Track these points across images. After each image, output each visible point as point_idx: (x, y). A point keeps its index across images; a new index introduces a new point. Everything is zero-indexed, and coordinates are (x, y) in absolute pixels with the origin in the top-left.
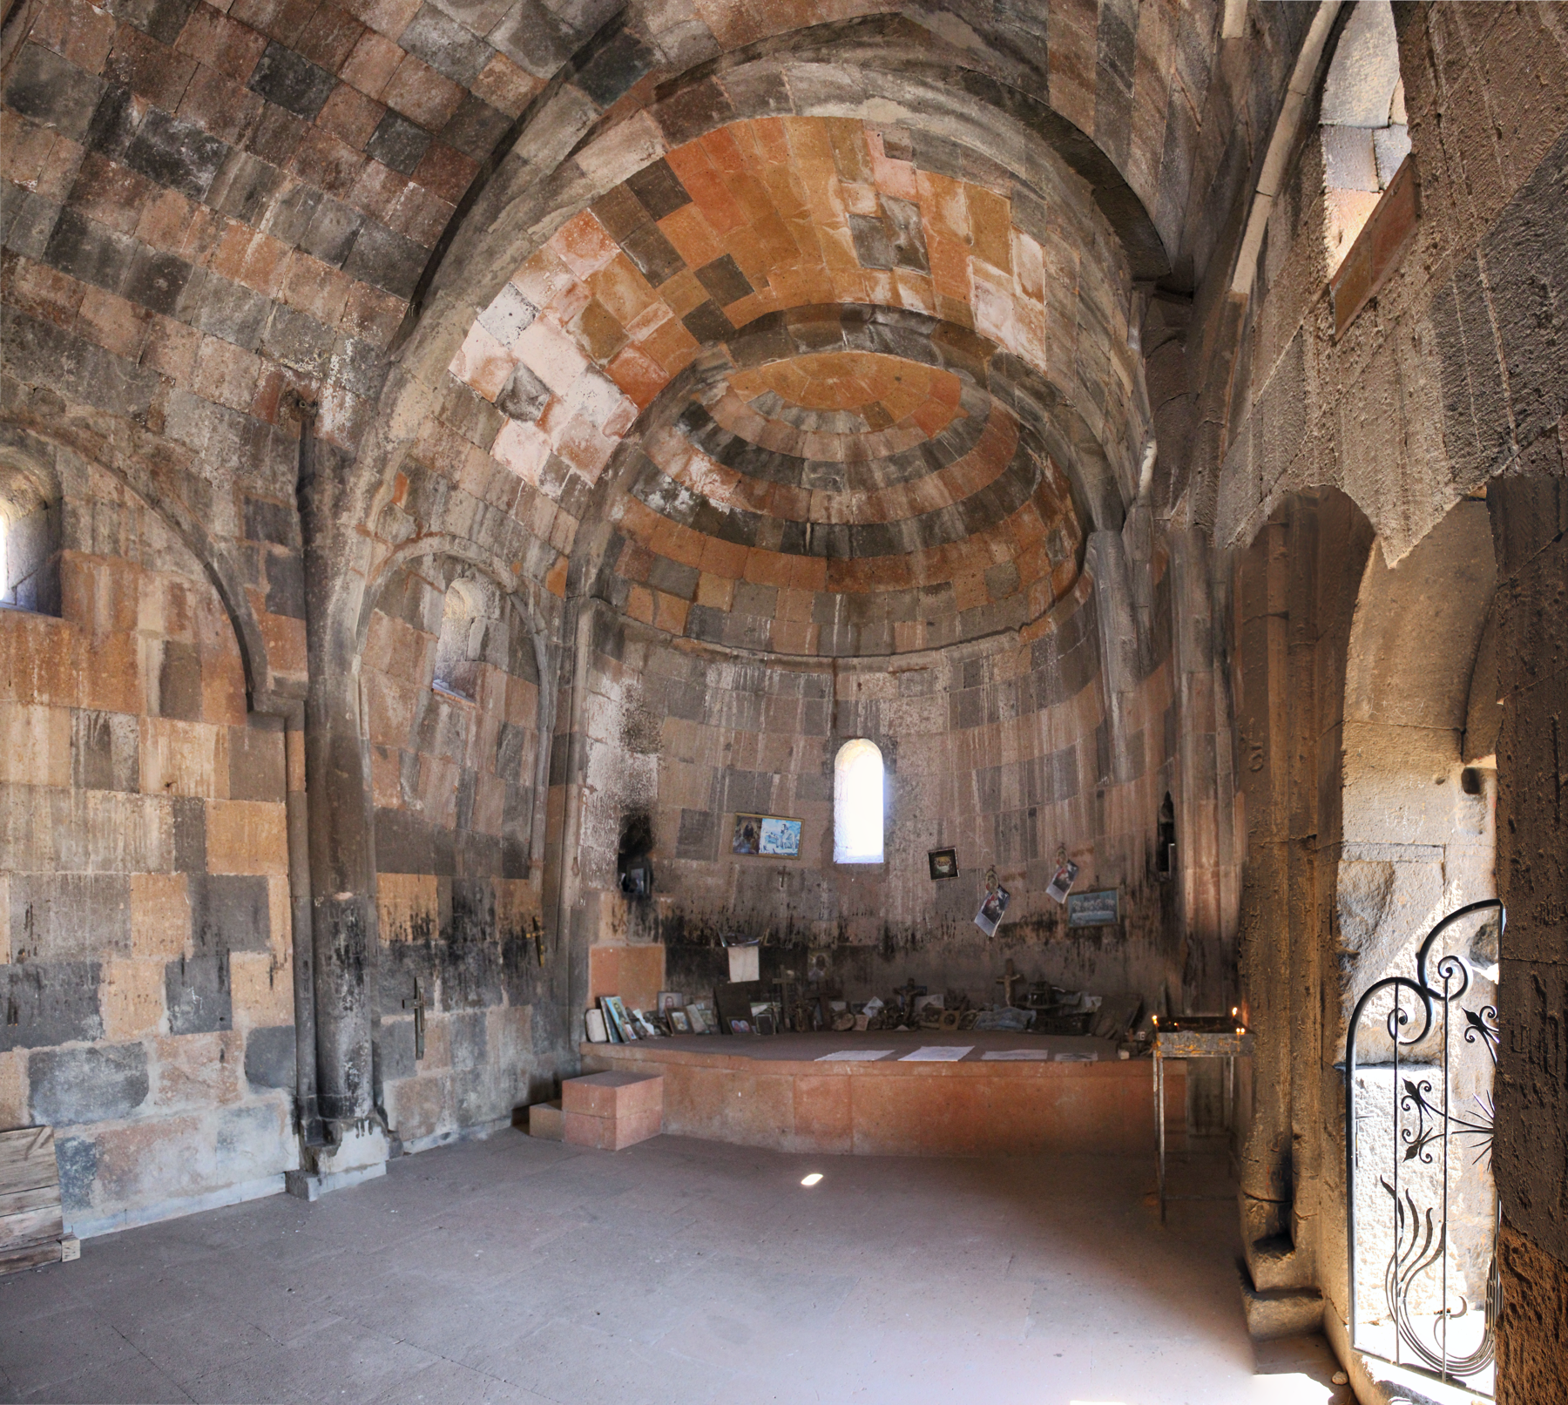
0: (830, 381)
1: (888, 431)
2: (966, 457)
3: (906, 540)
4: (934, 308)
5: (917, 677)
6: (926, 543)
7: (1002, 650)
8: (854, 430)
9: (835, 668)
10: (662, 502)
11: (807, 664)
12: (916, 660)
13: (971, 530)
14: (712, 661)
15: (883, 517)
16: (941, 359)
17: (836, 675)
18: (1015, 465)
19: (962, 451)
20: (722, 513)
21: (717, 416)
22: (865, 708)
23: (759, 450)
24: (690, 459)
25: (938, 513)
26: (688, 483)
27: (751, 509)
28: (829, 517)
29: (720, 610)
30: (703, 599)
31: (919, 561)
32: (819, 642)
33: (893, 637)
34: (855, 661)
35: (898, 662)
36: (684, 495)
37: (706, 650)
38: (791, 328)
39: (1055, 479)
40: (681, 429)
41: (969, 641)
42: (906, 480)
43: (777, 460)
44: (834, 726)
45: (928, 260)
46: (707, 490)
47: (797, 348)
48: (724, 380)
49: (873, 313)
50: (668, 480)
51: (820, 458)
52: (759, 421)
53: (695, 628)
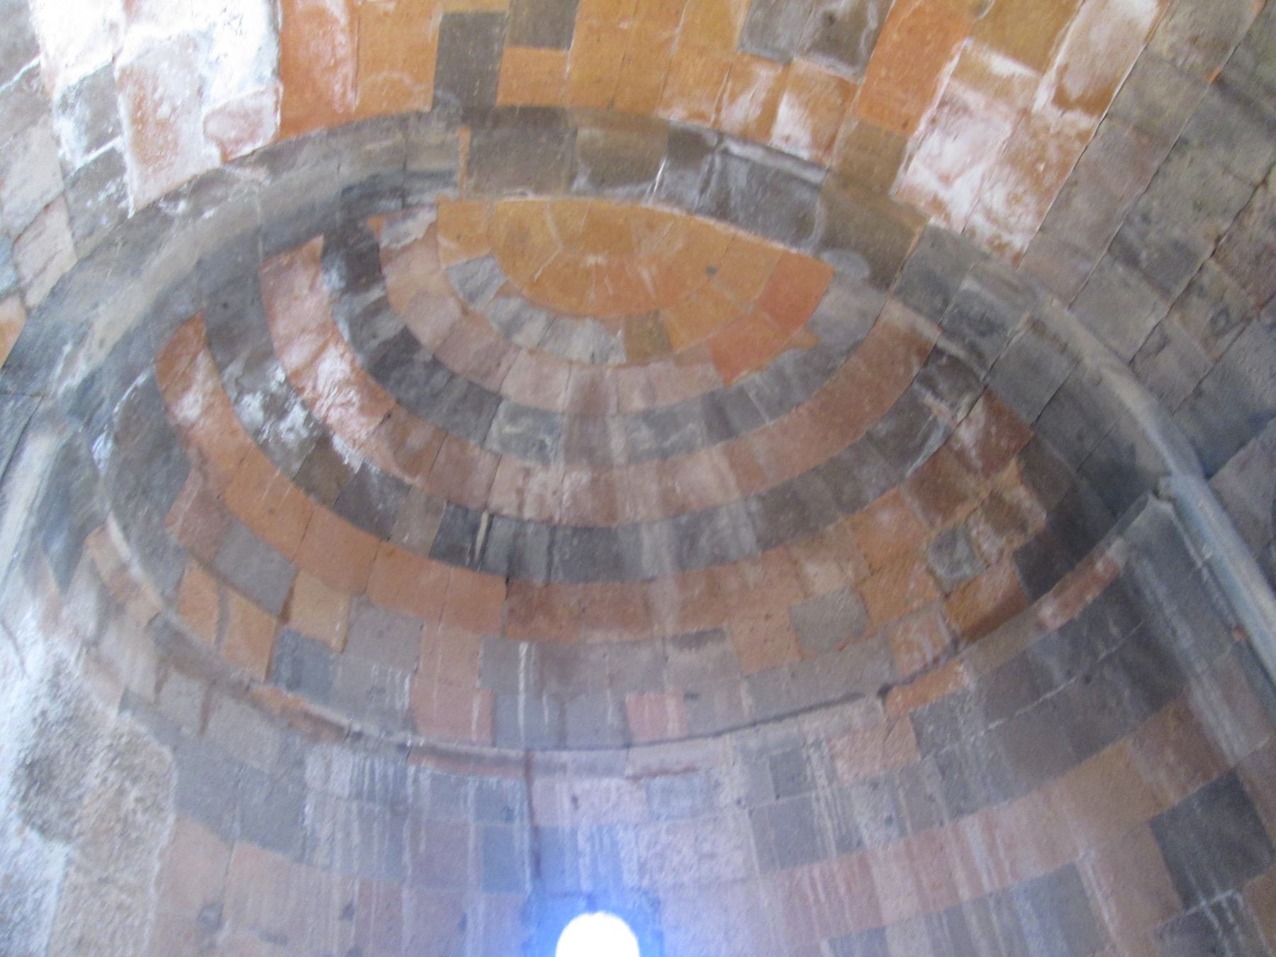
0: (591, 260)
1: (656, 367)
2: (785, 419)
3: (646, 559)
4: (829, 147)
5: (679, 784)
6: (682, 563)
7: (848, 730)
8: (597, 359)
9: (528, 766)
10: (260, 416)
11: (479, 759)
12: (676, 755)
13: (765, 543)
14: (315, 738)
15: (612, 516)
16: (818, 231)
17: (529, 781)
18: (882, 428)
19: (779, 406)
20: (348, 468)
21: (392, 276)
22: (591, 838)
23: (435, 364)
24: (323, 349)
25: (710, 513)
26: (307, 394)
27: (396, 472)
28: (520, 507)
29: (326, 645)
30: (297, 622)
31: (667, 595)
32: (496, 727)
33: (625, 718)
34: (565, 756)
35: (642, 757)
36: (297, 415)
37: (307, 715)
38: (584, 133)
39: (984, 442)
40: (331, 280)
41: (779, 718)
42: (664, 455)
43: (458, 390)
44: (537, 872)
45: (873, 43)
46: (334, 416)
47: (572, 178)
48: (434, 206)
49: (720, 141)
50: (280, 376)
51: (529, 400)
52: (453, 308)
53: (286, 672)
